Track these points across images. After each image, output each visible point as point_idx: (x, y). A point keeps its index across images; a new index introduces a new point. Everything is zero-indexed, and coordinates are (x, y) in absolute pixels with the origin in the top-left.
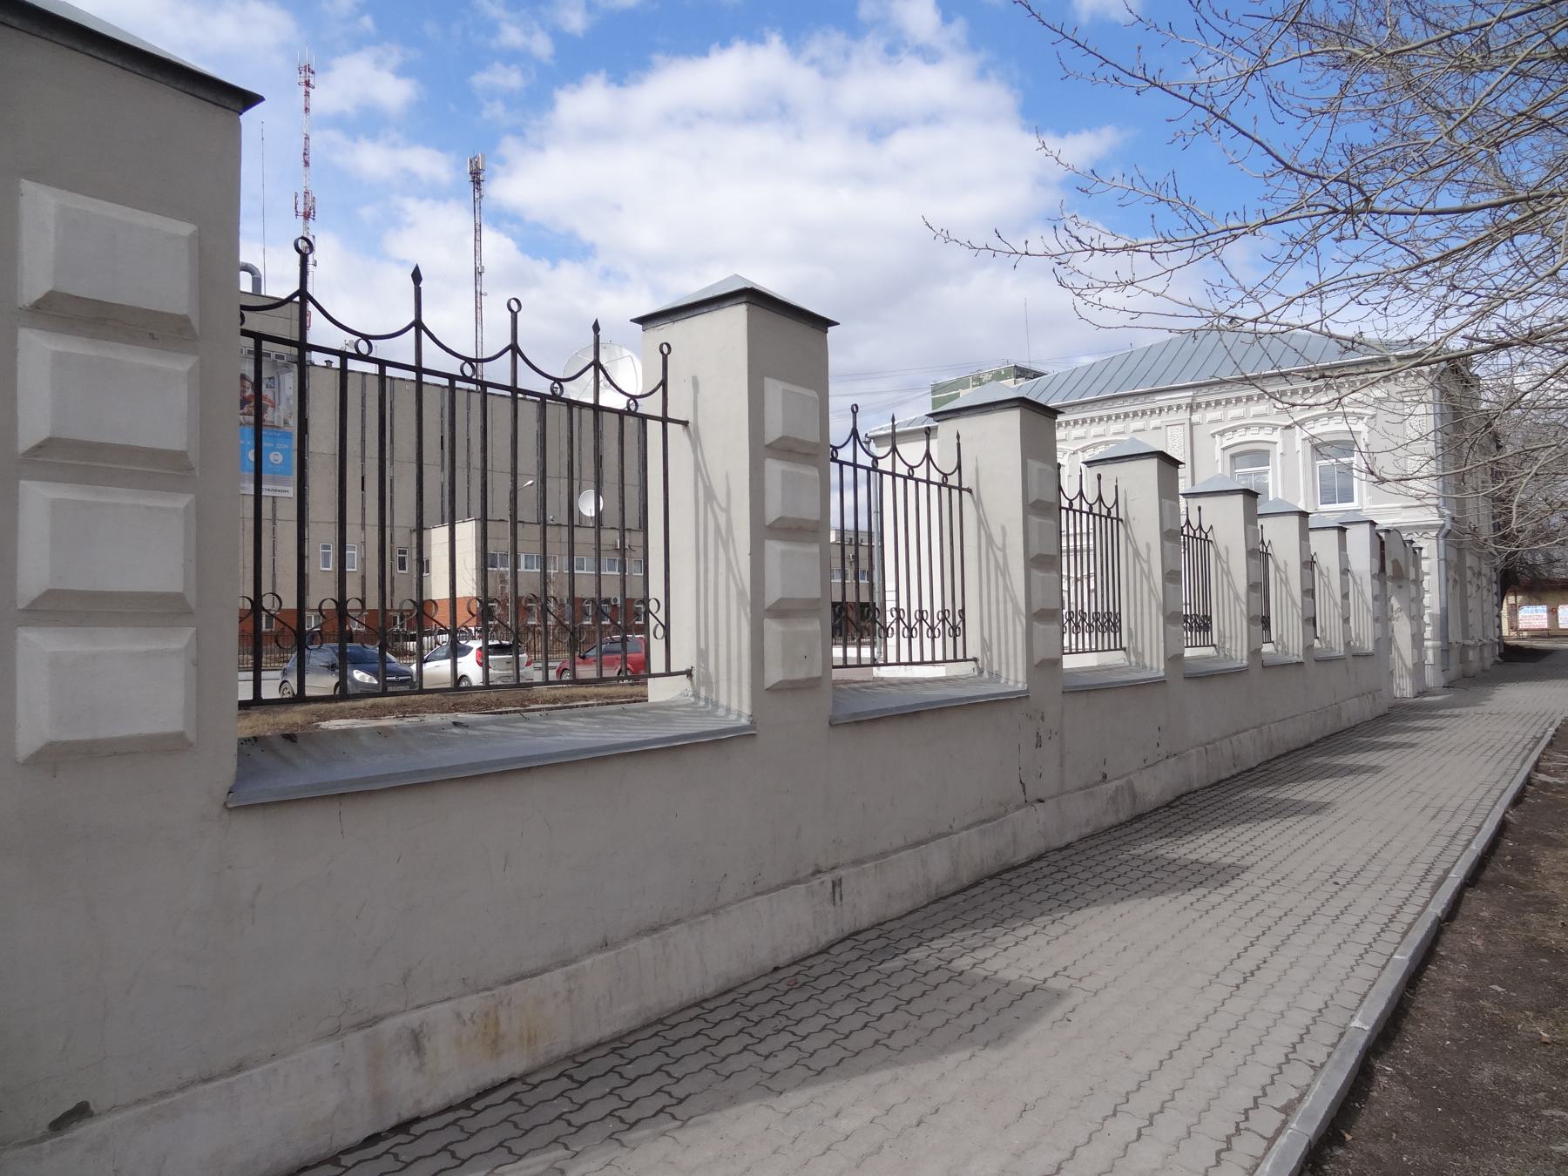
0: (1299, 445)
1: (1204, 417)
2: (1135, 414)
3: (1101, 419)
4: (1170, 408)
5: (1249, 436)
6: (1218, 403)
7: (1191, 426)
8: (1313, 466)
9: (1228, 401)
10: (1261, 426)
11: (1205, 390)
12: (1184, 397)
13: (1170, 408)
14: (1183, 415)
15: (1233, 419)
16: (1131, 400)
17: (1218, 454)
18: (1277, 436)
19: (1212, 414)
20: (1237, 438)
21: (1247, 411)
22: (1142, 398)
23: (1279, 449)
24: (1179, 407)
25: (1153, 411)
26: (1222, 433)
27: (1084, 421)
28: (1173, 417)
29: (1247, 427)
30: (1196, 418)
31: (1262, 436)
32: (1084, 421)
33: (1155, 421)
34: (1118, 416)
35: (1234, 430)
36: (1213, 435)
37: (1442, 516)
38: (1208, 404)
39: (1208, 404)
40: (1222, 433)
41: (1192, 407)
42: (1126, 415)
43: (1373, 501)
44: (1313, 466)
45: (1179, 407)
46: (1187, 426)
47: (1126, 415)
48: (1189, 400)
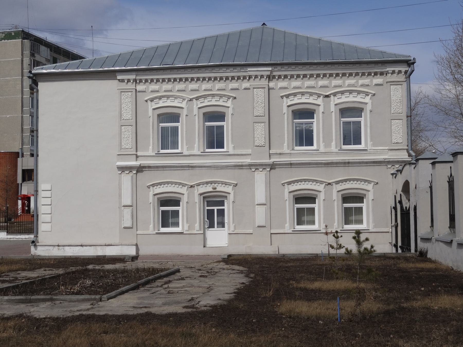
0: (333, 108)
1: (276, 85)
2: (233, 78)
3: (210, 79)
4: (256, 77)
5: (304, 100)
6: (286, 77)
7: (269, 89)
8: (340, 120)
9: (292, 76)
10: (311, 94)
11: (279, 68)
13: (256, 77)
14: (264, 82)
15: (295, 88)
17: (285, 109)
18: (320, 101)
19: (282, 83)
20: (296, 101)
21: (303, 84)
22: (239, 68)
23: (321, 109)
24: (262, 76)
25: (244, 78)
26: (287, 96)
27: (198, 79)
28: (257, 82)
29: (303, 94)
30: (272, 84)
31: (311, 100)
32: (198, 79)
33: (246, 84)
34: (221, 78)
35: (295, 95)
36: (282, 97)
37: (410, 155)
38: (280, 77)
39: (280, 77)
40: (287, 96)
41: (270, 78)
42: (239, 78)
43: (374, 145)
44: (340, 120)
45: (262, 76)
46: (267, 90)
47: (227, 78)
48: (269, 73)
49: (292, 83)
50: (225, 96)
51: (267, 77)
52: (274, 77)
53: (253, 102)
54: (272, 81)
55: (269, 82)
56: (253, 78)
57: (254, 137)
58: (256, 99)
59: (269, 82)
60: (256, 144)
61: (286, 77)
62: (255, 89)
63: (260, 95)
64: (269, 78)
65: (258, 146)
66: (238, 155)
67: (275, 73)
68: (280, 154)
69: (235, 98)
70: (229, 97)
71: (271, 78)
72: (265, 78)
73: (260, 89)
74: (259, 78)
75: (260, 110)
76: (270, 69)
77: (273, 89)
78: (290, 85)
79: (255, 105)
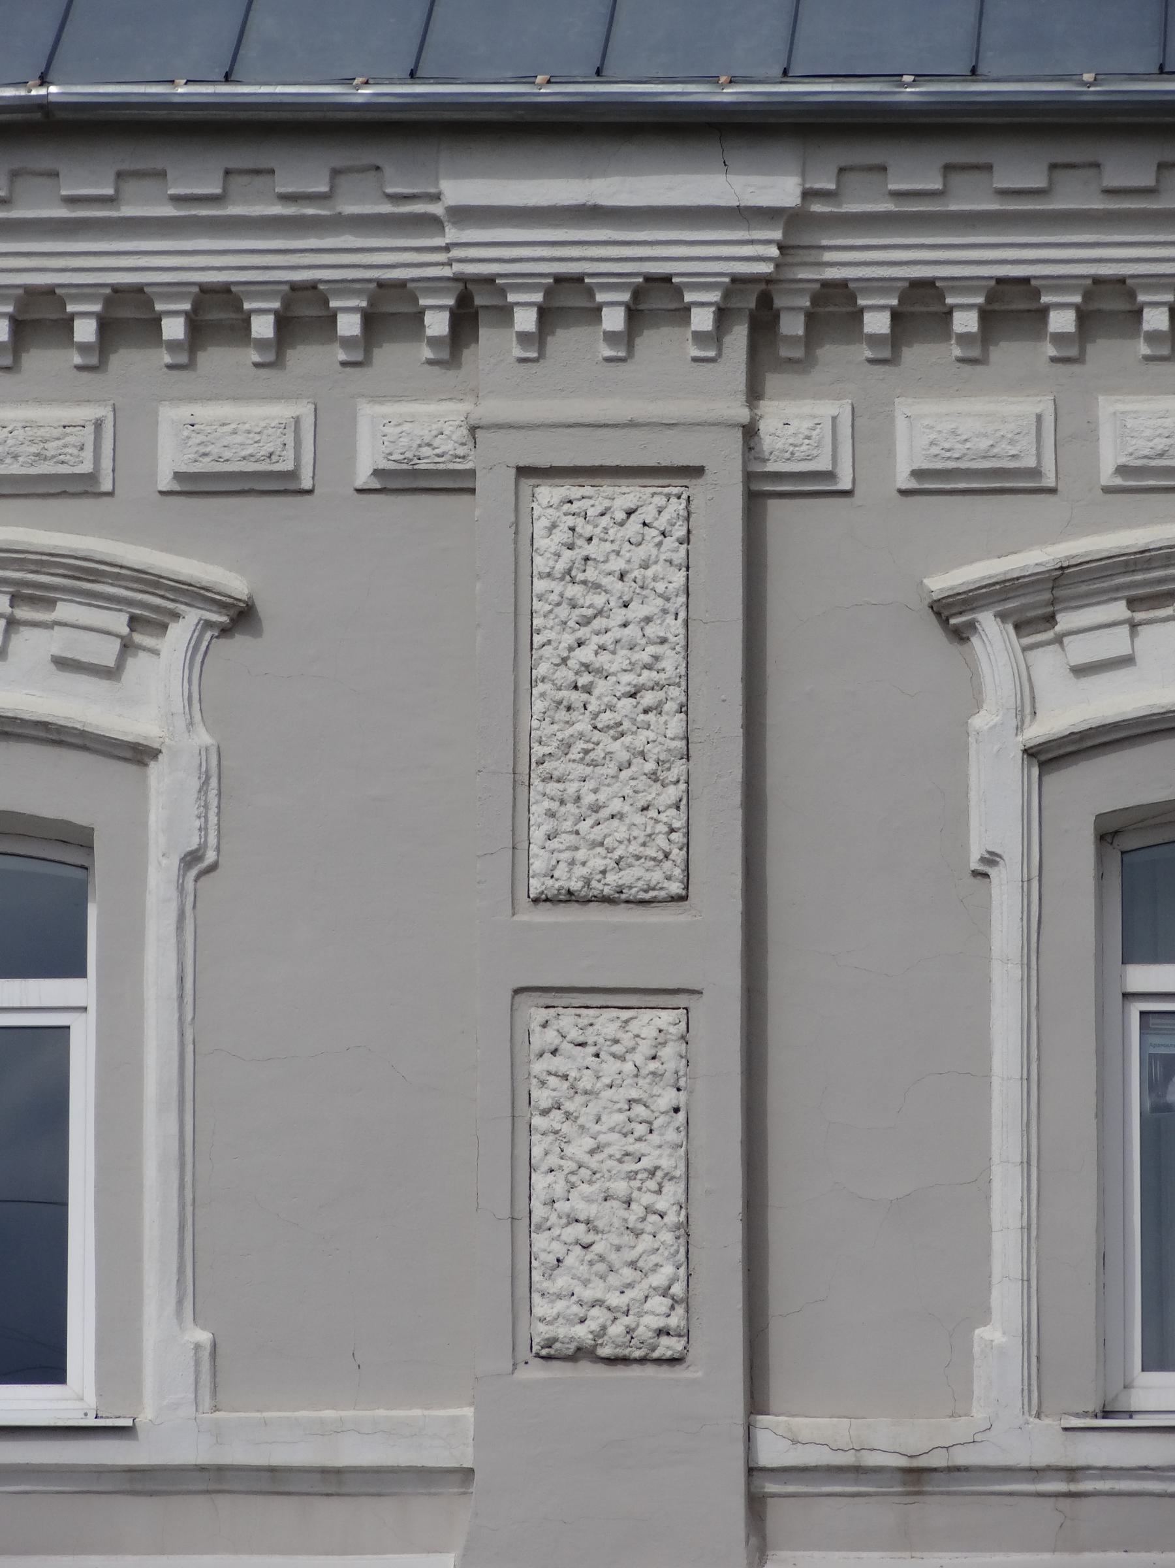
1: (870, 430)
2: (216, 314)
4: (566, 301)
6: (1012, 307)
11: (915, 172)
12: (710, 214)
13: (566, 301)
14: (685, 387)
16: (196, 175)
17: (996, 805)
22: (304, 172)
24: (654, 300)
25: (390, 312)
26: (1036, 604)
28: (583, 390)
30: (801, 424)
33: (406, 416)
36: (953, 616)
38: (920, 308)
40: (1036, 604)
41: (775, 322)
42: (303, 314)
45: (654, 300)
47: (127, 316)
48: (753, 253)
49: (1108, 407)
50: (87, 577)
51: (723, 315)
52: (835, 308)
53: (522, 685)
54: (803, 365)
55: (754, 393)
56: (526, 320)
57: (520, 1222)
58: (554, 636)
59: (754, 393)
60: (555, 1316)
61: (1012, 307)
62: (548, 494)
63: (623, 577)
64: (764, 323)
65: (582, 1353)
66: (274, 1481)
67: (845, 259)
68: (916, 1477)
69: (241, 617)
70: (149, 603)
71: (793, 325)
72: (703, 320)
73: (627, 494)
74: (614, 320)
75: (619, 801)
76: (779, 188)
77: (818, 487)
78: (1073, 431)
79: (547, 732)
